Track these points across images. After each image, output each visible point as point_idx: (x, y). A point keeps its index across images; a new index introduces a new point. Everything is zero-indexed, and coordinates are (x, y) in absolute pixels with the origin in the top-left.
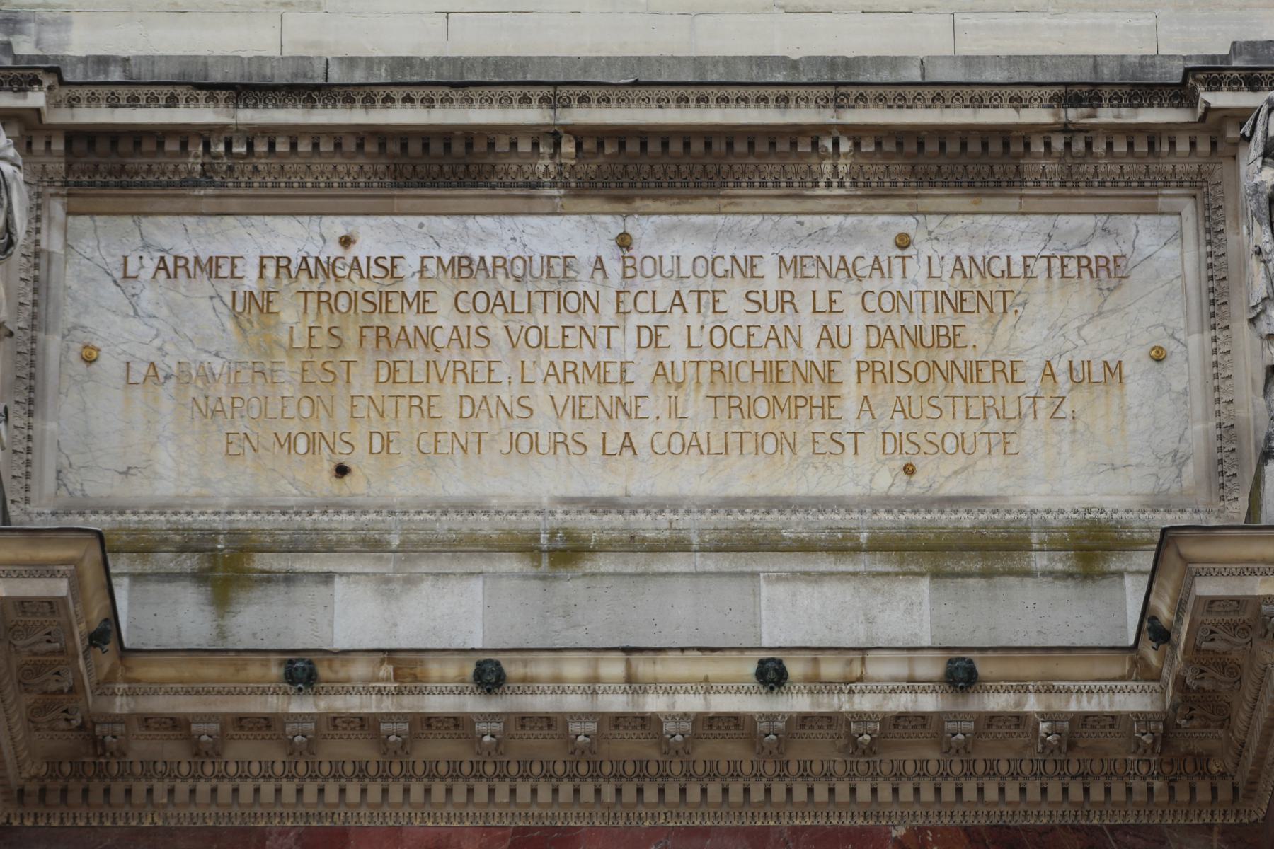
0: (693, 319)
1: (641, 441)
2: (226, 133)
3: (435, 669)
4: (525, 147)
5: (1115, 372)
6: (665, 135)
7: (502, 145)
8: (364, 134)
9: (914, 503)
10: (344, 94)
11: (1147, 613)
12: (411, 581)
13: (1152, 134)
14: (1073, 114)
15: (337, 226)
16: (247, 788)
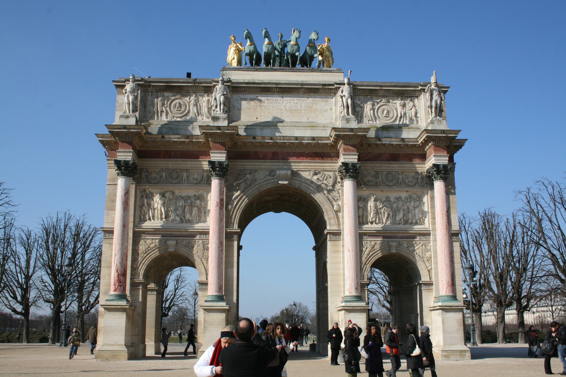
0: (289, 105)
1: (284, 116)
2: (247, 87)
3: (266, 137)
4: (274, 88)
5: (327, 110)
6: (286, 88)
7: (272, 88)
8: (259, 87)
9: (309, 122)
10: (258, 83)
11: (330, 134)
12: (263, 129)
13: (331, 89)
14: (324, 87)
15: (256, 95)
16: (249, 148)
